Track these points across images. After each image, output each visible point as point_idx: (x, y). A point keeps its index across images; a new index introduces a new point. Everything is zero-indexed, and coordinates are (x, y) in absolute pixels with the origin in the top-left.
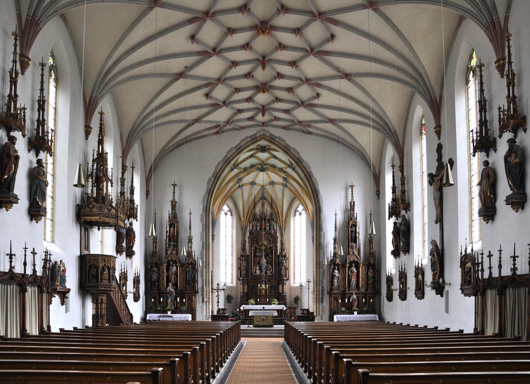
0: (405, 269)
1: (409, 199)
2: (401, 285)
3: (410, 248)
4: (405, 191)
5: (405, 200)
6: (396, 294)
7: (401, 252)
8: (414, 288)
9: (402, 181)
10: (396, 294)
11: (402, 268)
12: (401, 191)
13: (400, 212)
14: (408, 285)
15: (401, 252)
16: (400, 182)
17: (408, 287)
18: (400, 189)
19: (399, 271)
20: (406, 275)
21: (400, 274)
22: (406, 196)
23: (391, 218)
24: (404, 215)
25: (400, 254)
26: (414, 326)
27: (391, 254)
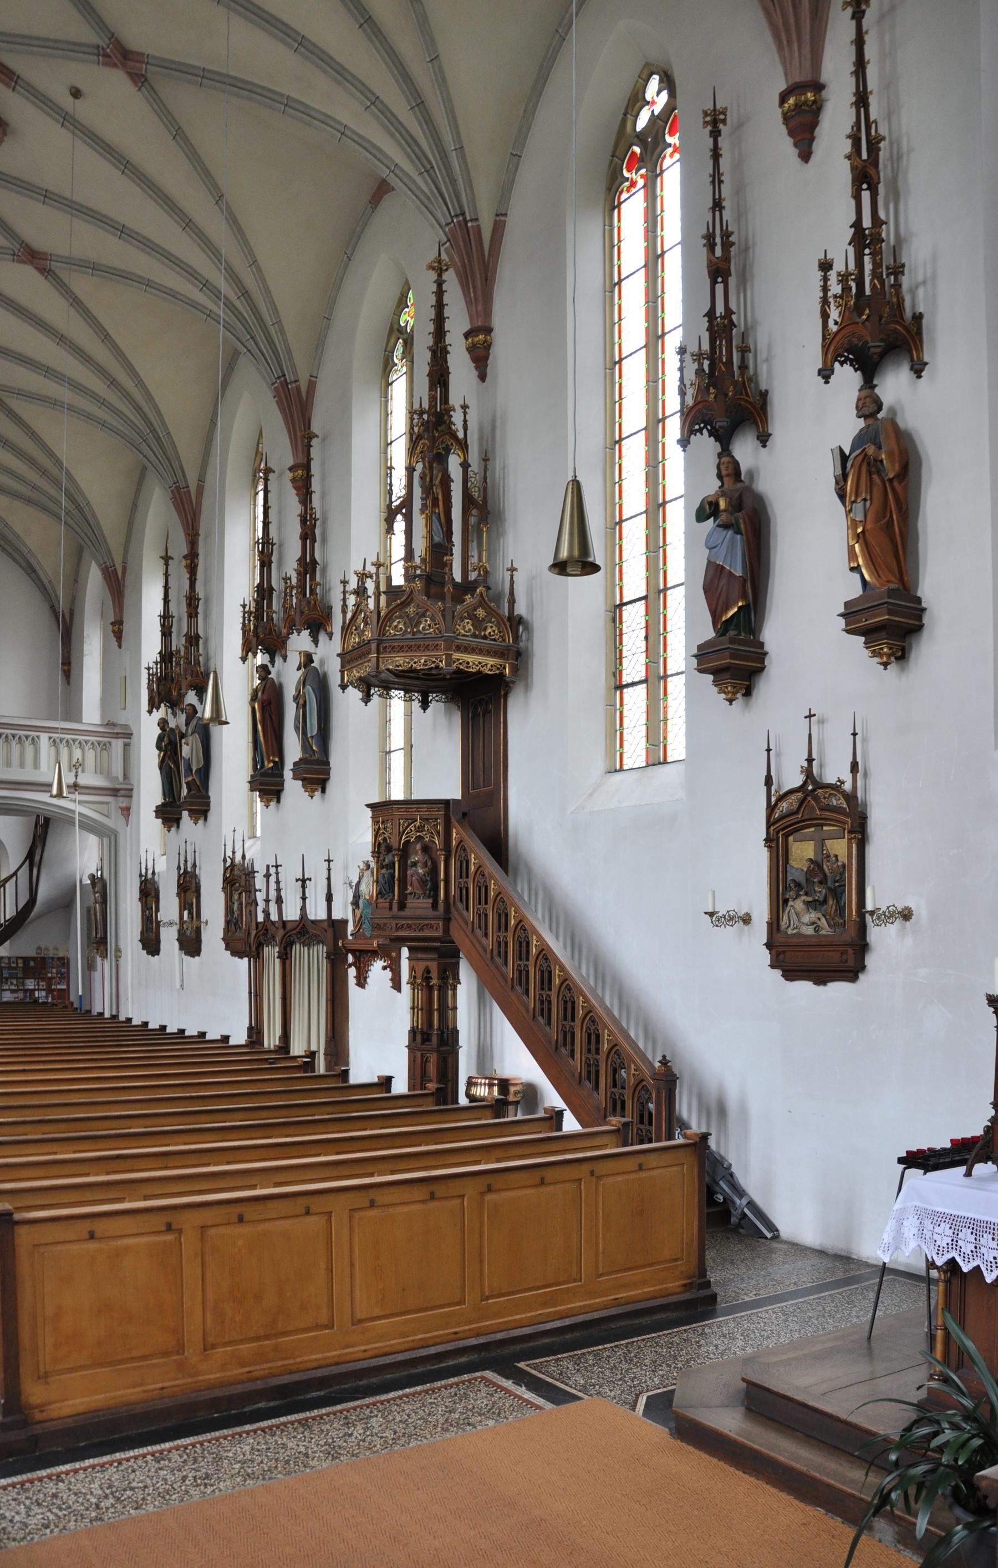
0: (194, 865)
1: (207, 660)
2: (186, 913)
3: (208, 804)
4: (198, 637)
5: (199, 662)
6: (169, 937)
7: (185, 814)
8: (222, 924)
9: (189, 605)
10: (169, 937)
11: (186, 861)
12: (258, 586)
13: (181, 697)
14: (205, 915)
15: (185, 814)
16: (184, 608)
17: (203, 919)
18: (185, 630)
19: (179, 868)
20: (199, 881)
21: (180, 876)
22: (201, 651)
23: (154, 710)
24: (193, 706)
25: (181, 818)
26: (176, 1031)
27: (154, 814)
